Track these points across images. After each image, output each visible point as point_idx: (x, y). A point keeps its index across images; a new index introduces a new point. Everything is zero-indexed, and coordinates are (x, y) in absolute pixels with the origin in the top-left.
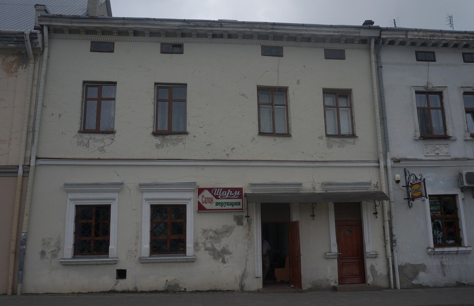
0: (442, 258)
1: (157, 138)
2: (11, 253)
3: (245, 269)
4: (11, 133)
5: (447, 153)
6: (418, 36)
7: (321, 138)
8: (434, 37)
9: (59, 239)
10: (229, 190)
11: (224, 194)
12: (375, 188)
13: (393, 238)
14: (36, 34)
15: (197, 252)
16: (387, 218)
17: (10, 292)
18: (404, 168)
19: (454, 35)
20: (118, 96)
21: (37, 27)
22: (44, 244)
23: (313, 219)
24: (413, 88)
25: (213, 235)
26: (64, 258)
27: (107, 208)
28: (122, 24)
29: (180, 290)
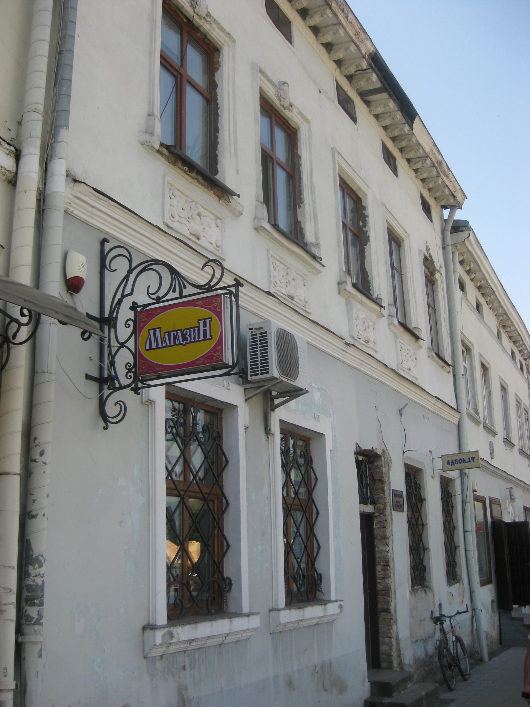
18: (102, 236)
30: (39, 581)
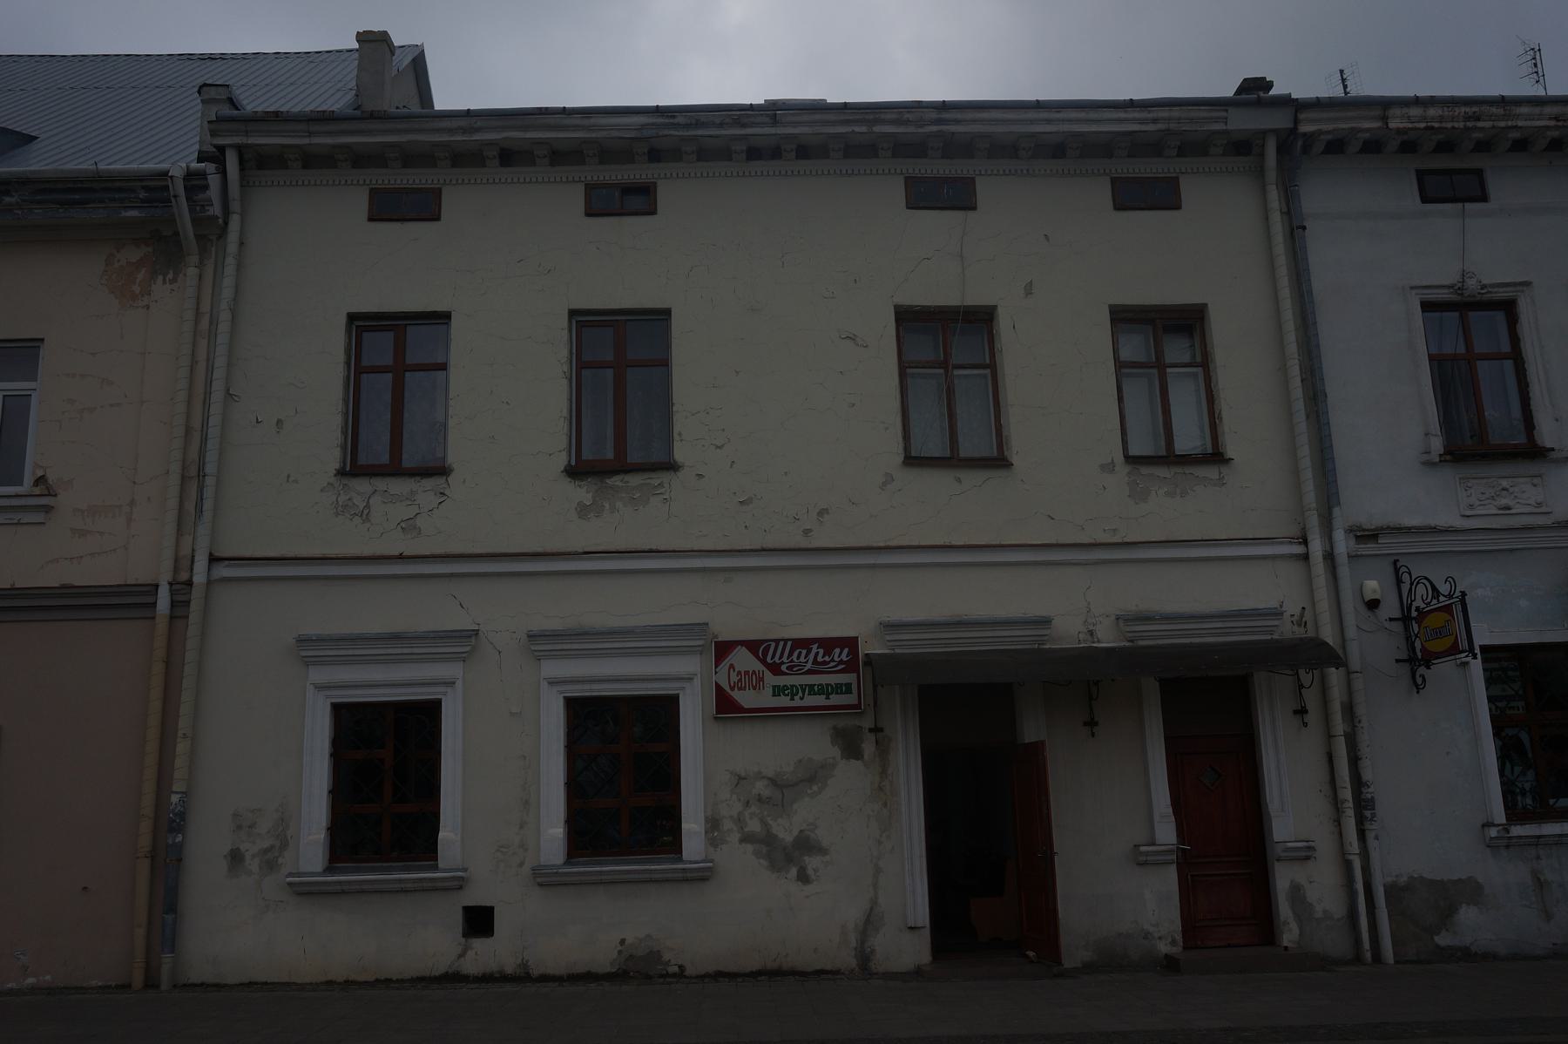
0: (1538, 858)
1: (580, 486)
2: (138, 858)
3: (874, 902)
4: (134, 483)
5: (1539, 504)
6: (1424, 119)
7: (1109, 468)
8: (1478, 119)
9: (283, 813)
10: (815, 646)
11: (798, 657)
12: (1296, 628)
13: (1362, 793)
14: (202, 175)
15: (716, 846)
16: (1339, 727)
17: (138, 980)
18: (1392, 559)
19: (1548, 110)
20: (458, 357)
21: (207, 152)
22: (239, 827)
23: (1093, 735)
24: (1414, 292)
25: (766, 793)
26: (299, 873)
27: (431, 710)
28: (464, 131)
29: (665, 972)
30: (1369, 796)
